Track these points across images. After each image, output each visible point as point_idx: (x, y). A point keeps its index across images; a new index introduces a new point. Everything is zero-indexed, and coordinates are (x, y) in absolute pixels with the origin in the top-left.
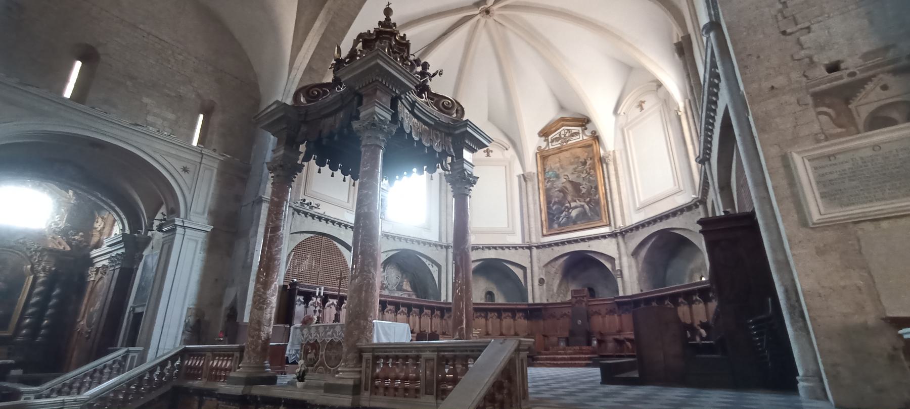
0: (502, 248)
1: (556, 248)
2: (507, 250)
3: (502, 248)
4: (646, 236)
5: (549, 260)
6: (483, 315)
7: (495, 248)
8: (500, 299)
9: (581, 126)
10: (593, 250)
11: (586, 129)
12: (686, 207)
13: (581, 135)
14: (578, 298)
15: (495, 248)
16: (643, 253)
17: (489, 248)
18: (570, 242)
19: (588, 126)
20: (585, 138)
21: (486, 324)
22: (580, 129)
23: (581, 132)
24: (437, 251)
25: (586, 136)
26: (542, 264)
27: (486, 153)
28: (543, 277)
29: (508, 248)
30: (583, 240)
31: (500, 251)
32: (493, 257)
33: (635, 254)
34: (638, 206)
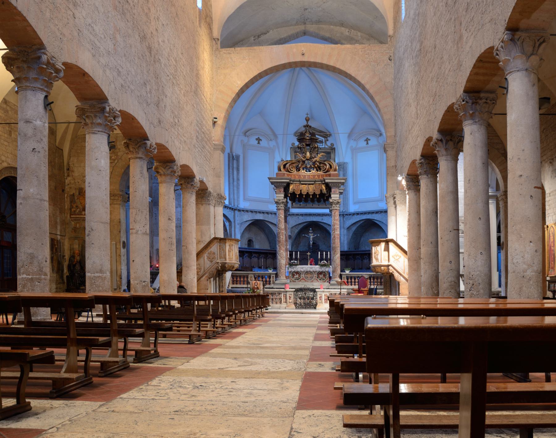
0: (268, 213)
1: (301, 217)
2: (270, 215)
3: (268, 213)
4: (359, 220)
5: (295, 225)
6: (256, 256)
7: (263, 213)
8: (257, 246)
9: (325, 137)
10: (325, 222)
11: (328, 140)
12: (384, 211)
13: (324, 144)
14: (313, 250)
15: (263, 213)
16: (354, 228)
17: (260, 212)
18: (310, 215)
19: (329, 138)
20: (326, 147)
21: (258, 262)
22: (323, 139)
23: (324, 141)
24: (230, 212)
25: (327, 145)
26: (291, 227)
27: (257, 141)
28: (290, 234)
29: (271, 213)
30: (319, 215)
31: (266, 215)
32: (261, 218)
33: (349, 228)
34: (355, 201)
